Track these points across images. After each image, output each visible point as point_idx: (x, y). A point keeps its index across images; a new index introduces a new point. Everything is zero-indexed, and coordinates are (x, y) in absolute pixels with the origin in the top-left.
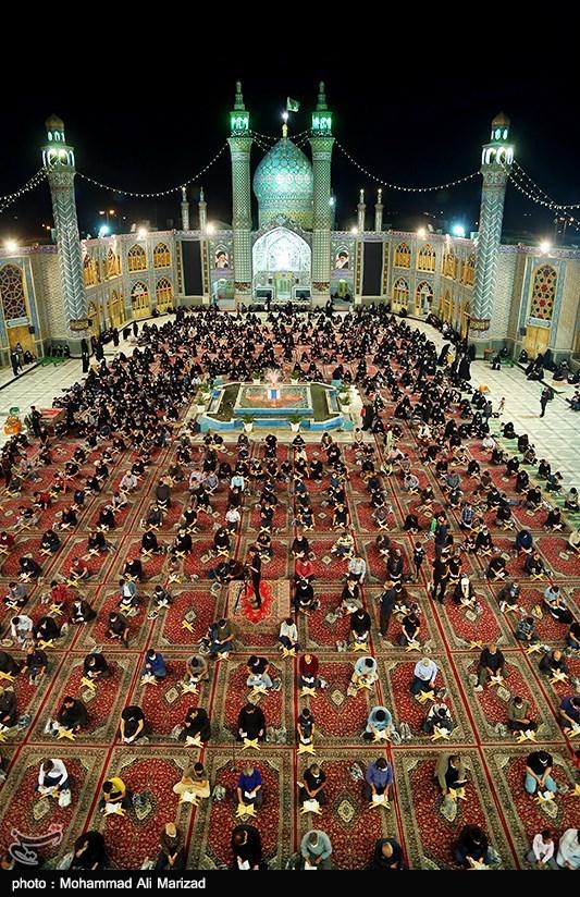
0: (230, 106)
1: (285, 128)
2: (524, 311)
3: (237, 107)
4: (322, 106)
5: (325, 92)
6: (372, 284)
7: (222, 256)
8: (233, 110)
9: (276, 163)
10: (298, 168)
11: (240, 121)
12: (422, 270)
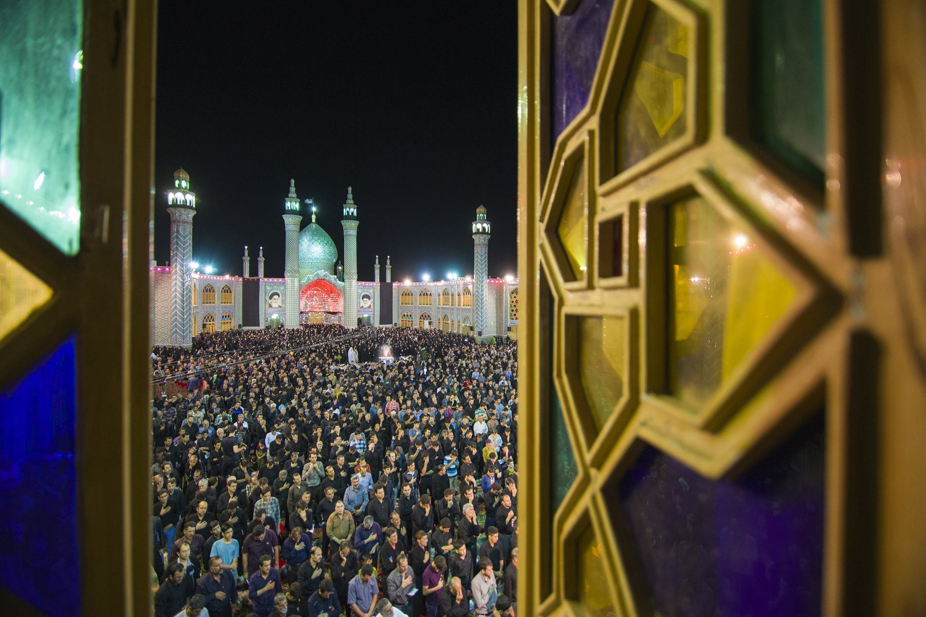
0: (286, 194)
1: (314, 217)
2: (506, 316)
3: (290, 195)
4: (352, 202)
6: (386, 316)
7: (276, 297)
9: (309, 237)
11: (293, 204)
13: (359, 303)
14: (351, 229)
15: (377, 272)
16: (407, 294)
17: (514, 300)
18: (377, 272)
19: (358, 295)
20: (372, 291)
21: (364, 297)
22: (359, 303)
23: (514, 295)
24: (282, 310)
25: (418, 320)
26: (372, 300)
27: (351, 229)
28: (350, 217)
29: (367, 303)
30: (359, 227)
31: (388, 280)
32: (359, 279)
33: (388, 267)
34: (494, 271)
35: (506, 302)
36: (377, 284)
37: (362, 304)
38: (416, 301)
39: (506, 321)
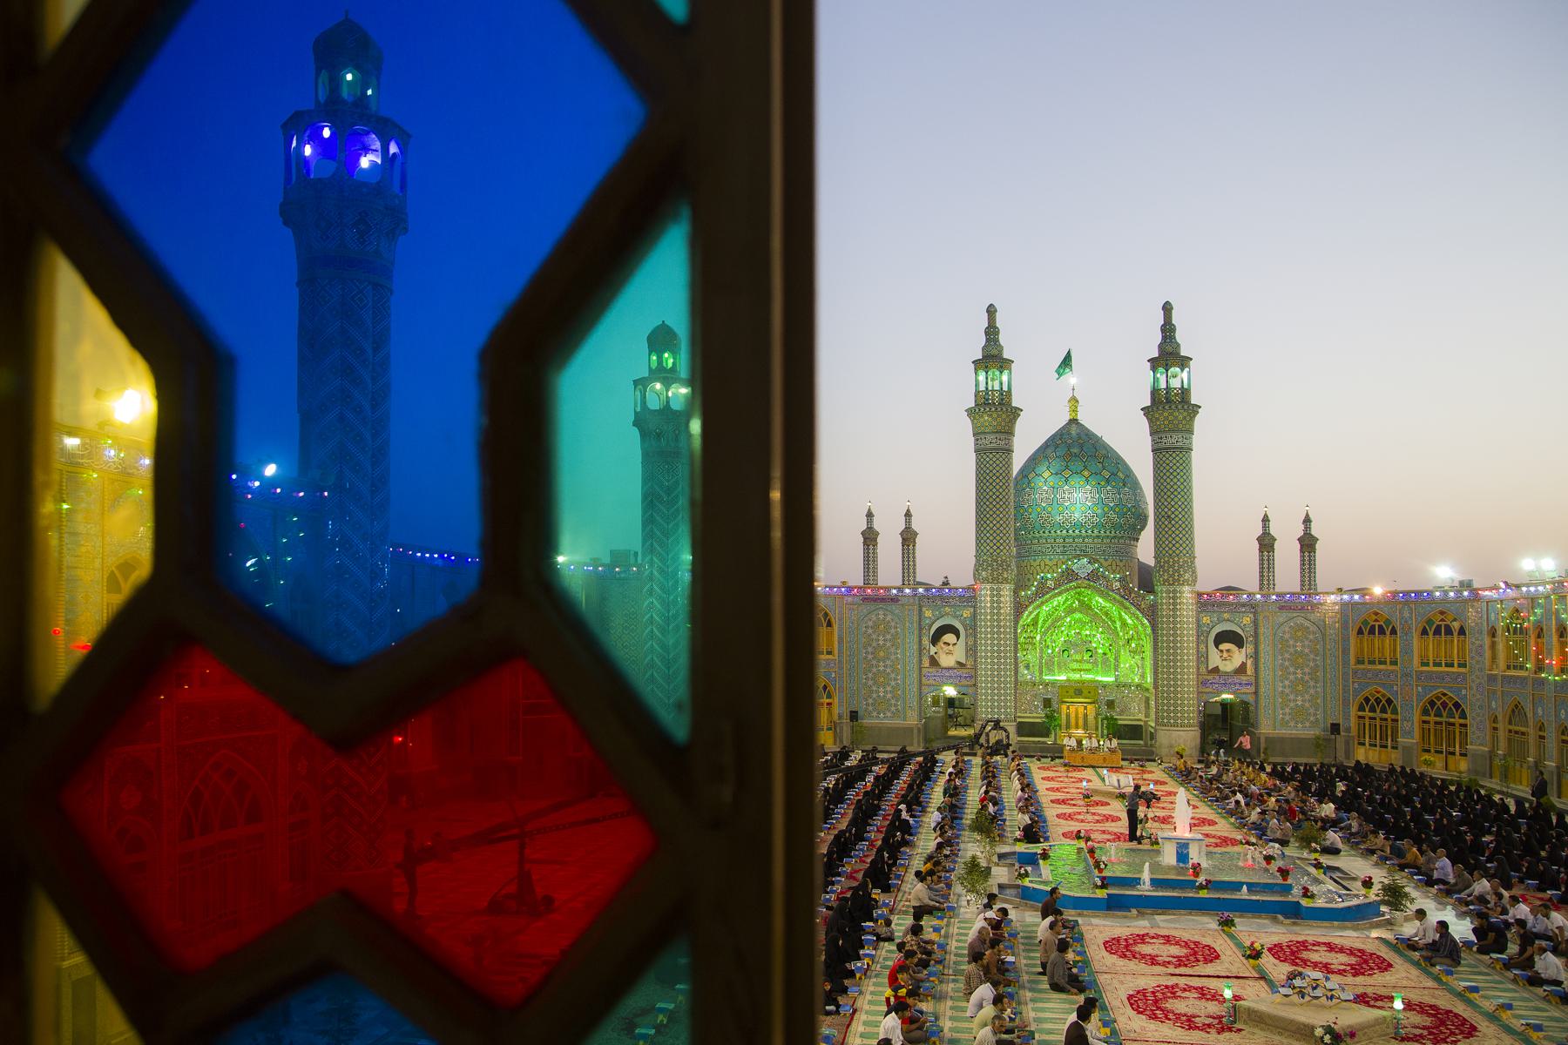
12: (1431, 668)
13: (1202, 658)
19: (1201, 634)
20: (1247, 620)
21: (1221, 638)
22: (1202, 658)
24: (966, 672)
25: (1416, 716)
37: (1215, 659)
38: (1407, 650)
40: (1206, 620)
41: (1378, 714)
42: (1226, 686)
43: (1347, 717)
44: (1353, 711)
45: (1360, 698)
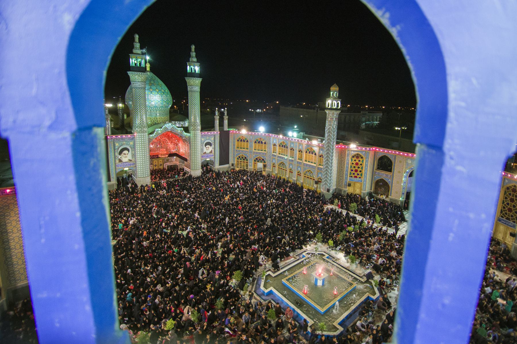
2: (347, 175)
3: (135, 51)
4: (195, 60)
5: (195, 51)
6: (224, 159)
8: (132, 53)
10: (163, 91)
13: (202, 150)
14: (195, 86)
15: (217, 122)
16: (242, 140)
17: (354, 162)
18: (217, 122)
19: (202, 143)
20: (213, 139)
22: (202, 150)
23: (355, 158)
26: (213, 146)
27: (195, 86)
28: (193, 75)
29: (209, 149)
30: (202, 83)
31: (226, 128)
32: (203, 129)
33: (226, 117)
34: (342, 138)
35: (348, 164)
36: (216, 132)
37: (205, 150)
39: (347, 178)
40: (203, 139)
41: (242, 161)
42: (208, 157)
43: (234, 161)
44: (236, 160)
45: (238, 157)
